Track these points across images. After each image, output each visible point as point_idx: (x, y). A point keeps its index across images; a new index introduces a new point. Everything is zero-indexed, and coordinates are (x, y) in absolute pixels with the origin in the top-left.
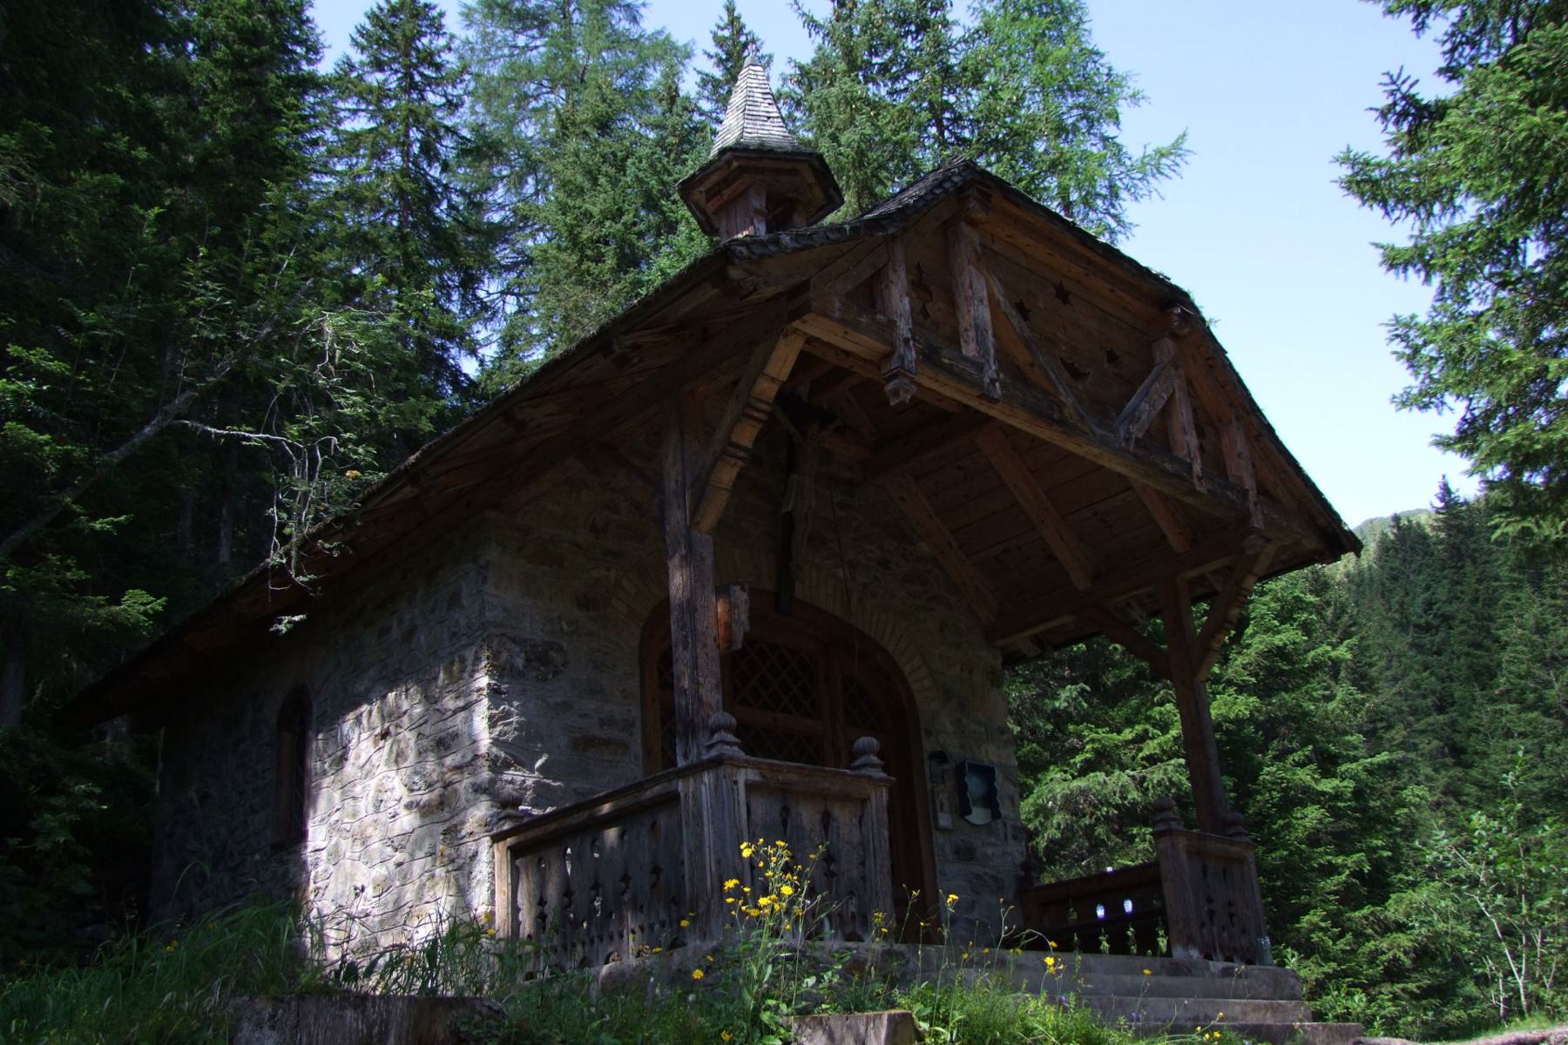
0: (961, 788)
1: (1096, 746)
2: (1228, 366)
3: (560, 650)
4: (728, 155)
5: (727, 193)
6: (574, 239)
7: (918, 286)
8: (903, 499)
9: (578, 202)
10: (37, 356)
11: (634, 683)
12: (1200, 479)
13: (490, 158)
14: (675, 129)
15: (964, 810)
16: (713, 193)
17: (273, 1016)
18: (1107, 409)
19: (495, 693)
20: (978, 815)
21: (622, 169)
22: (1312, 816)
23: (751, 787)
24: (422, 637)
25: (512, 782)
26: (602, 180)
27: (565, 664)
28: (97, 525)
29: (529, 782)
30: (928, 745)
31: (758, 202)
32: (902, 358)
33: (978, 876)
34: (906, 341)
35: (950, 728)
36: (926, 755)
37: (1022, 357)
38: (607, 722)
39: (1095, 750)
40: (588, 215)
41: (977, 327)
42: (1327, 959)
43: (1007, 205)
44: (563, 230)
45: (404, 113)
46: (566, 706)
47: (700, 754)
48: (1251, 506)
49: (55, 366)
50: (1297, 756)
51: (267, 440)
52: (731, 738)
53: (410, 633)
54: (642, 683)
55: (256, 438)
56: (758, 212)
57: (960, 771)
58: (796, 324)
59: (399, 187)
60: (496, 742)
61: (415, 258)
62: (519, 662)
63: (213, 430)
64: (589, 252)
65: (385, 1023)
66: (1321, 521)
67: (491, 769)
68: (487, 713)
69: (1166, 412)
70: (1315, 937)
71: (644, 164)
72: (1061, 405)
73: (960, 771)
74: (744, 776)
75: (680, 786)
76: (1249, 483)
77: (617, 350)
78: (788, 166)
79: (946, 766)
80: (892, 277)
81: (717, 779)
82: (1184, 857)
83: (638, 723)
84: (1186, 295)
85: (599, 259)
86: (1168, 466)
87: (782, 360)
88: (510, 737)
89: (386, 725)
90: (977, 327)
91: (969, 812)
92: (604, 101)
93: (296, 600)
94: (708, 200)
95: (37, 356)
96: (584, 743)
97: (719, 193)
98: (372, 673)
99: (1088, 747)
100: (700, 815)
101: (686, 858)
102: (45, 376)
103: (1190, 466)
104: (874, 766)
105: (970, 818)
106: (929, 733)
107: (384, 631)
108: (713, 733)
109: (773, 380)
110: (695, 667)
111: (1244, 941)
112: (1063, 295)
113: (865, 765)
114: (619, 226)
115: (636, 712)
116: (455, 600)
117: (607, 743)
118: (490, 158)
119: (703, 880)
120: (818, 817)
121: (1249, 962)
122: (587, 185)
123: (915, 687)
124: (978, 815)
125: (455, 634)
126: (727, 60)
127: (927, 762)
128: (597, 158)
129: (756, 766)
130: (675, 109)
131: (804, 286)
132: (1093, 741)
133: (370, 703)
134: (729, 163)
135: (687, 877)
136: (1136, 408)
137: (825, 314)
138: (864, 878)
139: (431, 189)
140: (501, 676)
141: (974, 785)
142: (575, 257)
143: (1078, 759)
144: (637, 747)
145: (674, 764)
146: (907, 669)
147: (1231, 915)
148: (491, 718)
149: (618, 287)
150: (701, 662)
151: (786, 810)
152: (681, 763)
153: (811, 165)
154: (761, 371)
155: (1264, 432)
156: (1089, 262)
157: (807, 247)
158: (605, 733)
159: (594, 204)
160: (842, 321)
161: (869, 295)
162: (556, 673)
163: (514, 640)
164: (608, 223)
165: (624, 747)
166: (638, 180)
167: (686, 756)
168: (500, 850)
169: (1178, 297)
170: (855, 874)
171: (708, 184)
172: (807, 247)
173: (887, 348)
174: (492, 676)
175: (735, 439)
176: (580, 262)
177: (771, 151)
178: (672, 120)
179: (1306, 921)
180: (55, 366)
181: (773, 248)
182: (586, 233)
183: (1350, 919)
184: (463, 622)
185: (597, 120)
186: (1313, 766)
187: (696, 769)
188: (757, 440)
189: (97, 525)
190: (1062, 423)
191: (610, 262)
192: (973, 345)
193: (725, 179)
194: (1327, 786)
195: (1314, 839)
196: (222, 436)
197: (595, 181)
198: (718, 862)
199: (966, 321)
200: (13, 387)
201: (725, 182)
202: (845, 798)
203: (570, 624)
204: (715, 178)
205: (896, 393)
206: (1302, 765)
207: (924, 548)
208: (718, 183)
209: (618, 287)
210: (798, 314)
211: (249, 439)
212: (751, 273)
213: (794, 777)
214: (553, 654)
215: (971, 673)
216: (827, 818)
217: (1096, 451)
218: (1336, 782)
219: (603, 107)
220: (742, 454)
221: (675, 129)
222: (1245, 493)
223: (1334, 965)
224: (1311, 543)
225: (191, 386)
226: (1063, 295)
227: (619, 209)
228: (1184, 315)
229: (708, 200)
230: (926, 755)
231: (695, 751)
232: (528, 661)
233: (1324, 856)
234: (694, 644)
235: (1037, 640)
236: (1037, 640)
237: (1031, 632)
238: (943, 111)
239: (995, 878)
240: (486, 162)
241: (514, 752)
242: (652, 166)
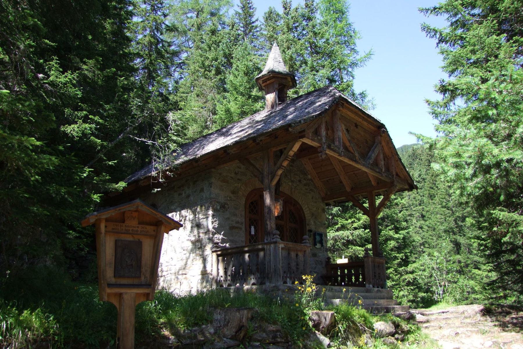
0: (315, 239)
1: (342, 223)
2: (392, 143)
3: (228, 204)
5: (268, 82)
6: (203, 64)
7: (327, 129)
8: (305, 164)
9: (205, 54)
10: (97, 118)
11: (243, 213)
13: (175, 31)
14: (233, 35)
15: (315, 244)
16: (264, 82)
17: (220, 312)
18: (364, 156)
19: (213, 216)
20: (318, 246)
21: (218, 46)
22: (392, 244)
23: (282, 248)
24: (192, 198)
25: (216, 238)
26: (212, 48)
27: (228, 208)
28: (110, 163)
29: (220, 238)
31: (276, 86)
32: (323, 147)
33: (317, 261)
34: (324, 143)
35: (313, 223)
36: (307, 230)
37: (348, 144)
38: (237, 222)
39: (341, 225)
40: (208, 58)
41: (339, 138)
42: (393, 281)
43: (347, 105)
44: (201, 62)
45: (152, 19)
46: (228, 219)
47: (271, 240)
48: (395, 179)
49: (101, 121)
50: (390, 228)
51: (152, 143)
52: (278, 237)
53: (188, 196)
54: (245, 212)
55: (150, 142)
56: (276, 89)
57: (315, 235)
58: (301, 140)
59: (150, 41)
60: (214, 228)
61: (153, 61)
62: (219, 207)
63: (138, 139)
64: (207, 69)
65: (243, 315)
66: (409, 182)
67: (212, 234)
68: (211, 221)
69: (378, 156)
70: (391, 275)
71: (225, 45)
72: (355, 156)
73: (315, 235)
74: (281, 246)
75: (265, 247)
77: (257, 141)
79: (311, 233)
80: (322, 127)
81: (275, 246)
83: (244, 223)
84: (384, 125)
85: (210, 71)
86: (377, 170)
87: (296, 147)
88: (216, 226)
89: (181, 218)
90: (339, 138)
91: (316, 245)
92: (214, 25)
93: (159, 185)
94: (263, 83)
95: (97, 118)
96: (232, 228)
97: (266, 82)
98: (176, 204)
99: (340, 224)
100: (270, 254)
101: (266, 263)
102: (97, 123)
105: (316, 246)
106: (308, 225)
107: (180, 194)
108: (274, 235)
109: (293, 151)
111: (381, 283)
112: (356, 126)
113: (305, 243)
114: (217, 63)
115: (244, 220)
116: (202, 190)
117: (237, 228)
118: (175, 31)
119: (271, 269)
120: (295, 255)
121: (382, 288)
122: (208, 49)
123: (306, 213)
124: (318, 246)
125: (202, 199)
126: (243, 8)
127: (307, 232)
128: (211, 42)
130: (234, 29)
131: (304, 131)
132: (341, 222)
133: (176, 212)
135: (266, 268)
136: (371, 155)
137: (308, 138)
138: (304, 269)
139: (158, 40)
140: (214, 211)
141: (318, 238)
142: (203, 70)
143: (337, 226)
144: (244, 229)
145: (264, 241)
146: (304, 208)
147: (379, 276)
148: (212, 222)
149: (215, 80)
151: (289, 254)
152: (266, 241)
153: (291, 77)
154: (291, 149)
155: (399, 160)
156: (363, 118)
157: (306, 122)
158: (237, 225)
159: (210, 55)
160: (312, 140)
161: (317, 133)
162: (227, 210)
163: (217, 202)
164: (214, 62)
165: (241, 229)
166: (223, 50)
167: (267, 240)
168: (214, 255)
169: (382, 126)
170: (302, 268)
172: (306, 122)
173: (320, 145)
174: (212, 211)
175: (283, 164)
176: (205, 71)
177: (281, 73)
178: (232, 32)
179: (389, 271)
180: (101, 121)
181: (299, 124)
182: (207, 63)
183: (399, 270)
184: (204, 196)
185: (211, 30)
186: (394, 231)
187: (270, 243)
188: (287, 165)
189: (110, 163)
190: (356, 161)
191: (213, 72)
192: (338, 142)
194: (396, 236)
195: (392, 250)
196: (140, 140)
197: (210, 49)
198: (275, 266)
200: (90, 126)
201: (268, 79)
202: (301, 251)
203: (230, 198)
206: (390, 230)
207: (309, 177)
208: (266, 79)
209: (215, 80)
210: (302, 137)
211: (147, 142)
212: (294, 129)
214: (226, 206)
215: (318, 209)
216: (297, 255)
217: (362, 167)
218: (399, 235)
219: (213, 27)
220: (284, 168)
221: (233, 35)
222: (393, 176)
223: (395, 282)
224: (407, 187)
225: (131, 126)
226: (356, 126)
227: (217, 57)
228: (384, 132)
229: (263, 83)
230: (307, 230)
231: (269, 239)
232: (220, 207)
233: (394, 254)
235: (335, 202)
236: (335, 202)
237: (333, 200)
238: (313, 43)
239: (321, 261)
240: (173, 33)
241: (218, 231)
242: (227, 46)
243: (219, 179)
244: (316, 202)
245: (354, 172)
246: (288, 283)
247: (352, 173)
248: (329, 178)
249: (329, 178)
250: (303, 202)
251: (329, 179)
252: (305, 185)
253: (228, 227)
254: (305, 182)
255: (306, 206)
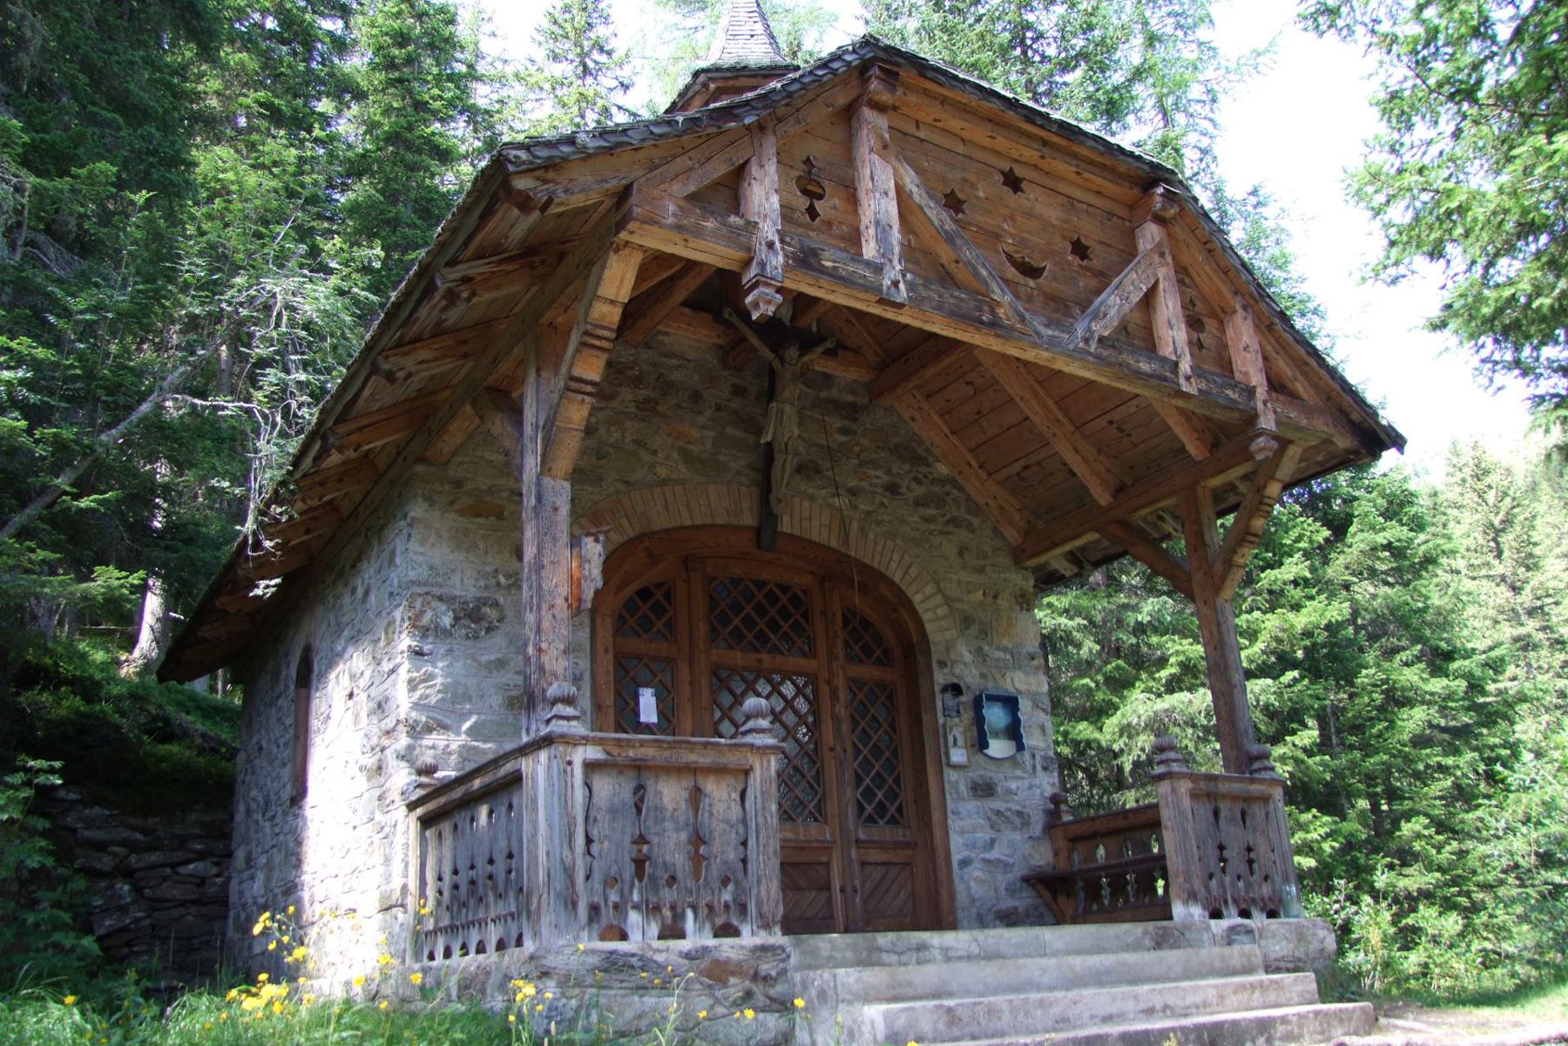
0: (979, 720)
1: (1181, 658)
3: (496, 604)
4: (702, 78)
12: (1188, 378)
15: (980, 743)
20: (998, 748)
22: (1414, 719)
23: (591, 767)
25: (433, 747)
29: (454, 746)
30: (940, 678)
32: (763, 265)
33: (998, 813)
35: (968, 657)
39: (1181, 664)
41: (877, 223)
42: (1430, 870)
47: (538, 730)
48: (1260, 406)
49: (41, 353)
50: (1404, 656)
51: (241, 408)
58: (623, 235)
60: (416, 706)
62: (447, 621)
66: (1355, 416)
70: (1417, 846)
72: (993, 305)
73: (977, 705)
76: (1258, 380)
82: (1187, 802)
88: (433, 700)
90: (877, 223)
91: (986, 746)
99: (1172, 660)
102: (36, 364)
103: (1176, 364)
104: (763, 731)
105: (989, 752)
106: (942, 664)
107: (354, 590)
109: (612, 302)
110: (539, 631)
111: (1266, 890)
112: (1013, 183)
120: (685, 794)
121: (1272, 914)
123: (926, 617)
124: (998, 748)
127: (939, 698)
129: (599, 742)
132: (1177, 653)
134: (705, 85)
141: (995, 716)
143: (1164, 674)
146: (916, 599)
147: (1250, 862)
148: (410, 681)
150: (545, 625)
151: (640, 789)
156: (1045, 143)
160: (678, 228)
162: (489, 630)
163: (440, 598)
173: (741, 255)
179: (1407, 829)
180: (41, 353)
183: (1462, 822)
186: (1423, 665)
189: (82, 505)
194: (1437, 685)
195: (1420, 741)
199: (867, 215)
202: (720, 771)
203: (508, 577)
205: (756, 305)
206: (1407, 664)
207: (942, 469)
211: (224, 408)
212: (545, 181)
213: (650, 752)
214: (487, 610)
215: (995, 597)
216: (696, 795)
217: (1045, 354)
218: (1444, 682)
220: (589, 389)
222: (1251, 392)
223: (1438, 875)
224: (1343, 442)
228: (1169, 197)
230: (937, 688)
232: (457, 619)
233: (1433, 755)
234: (539, 608)
235: (1073, 557)
236: (1073, 557)
239: (1019, 814)
243: (451, 503)
244: (981, 570)
245: (1108, 417)
246: (635, 935)
247: (1102, 422)
248: (1021, 463)
249: (1021, 463)
250: (913, 572)
251: (1026, 468)
252: (919, 503)
253: (496, 701)
254: (919, 491)
255: (929, 590)
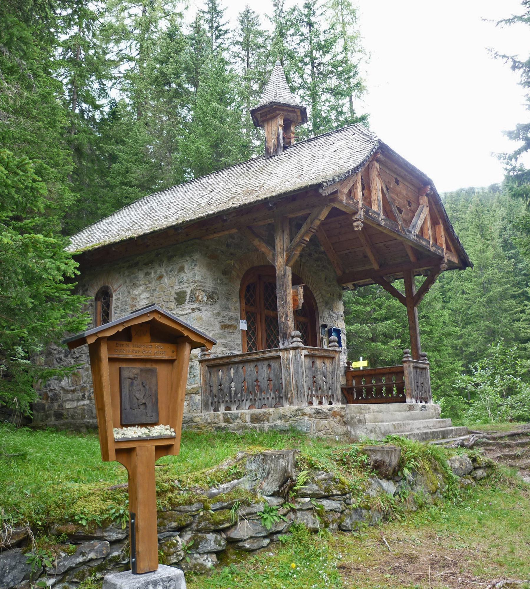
3: (216, 294)
4: (272, 104)
11: (238, 304)
12: (432, 247)
23: (305, 356)
30: (321, 323)
36: (320, 325)
38: (231, 319)
41: (378, 200)
46: (219, 314)
47: (288, 344)
52: (299, 340)
54: (240, 304)
74: (304, 352)
76: (444, 246)
78: (293, 109)
81: (296, 353)
90: (378, 200)
103: (429, 242)
104: (336, 346)
108: (293, 338)
109: (320, 220)
110: (287, 315)
123: (318, 301)
129: (307, 349)
134: (272, 106)
146: (315, 295)
150: (288, 313)
151: (313, 362)
152: (281, 347)
154: (316, 218)
162: (215, 302)
167: (283, 344)
171: (262, 112)
192: (376, 206)
193: (269, 111)
199: (374, 197)
204: (265, 110)
205: (357, 226)
207: (322, 249)
213: (316, 352)
214: (215, 295)
220: (306, 242)
222: (443, 250)
232: (208, 298)
234: (286, 307)
244: (330, 286)
245: (384, 243)
246: (314, 404)
247: (382, 244)
248: (349, 251)
249: (349, 251)
250: (314, 286)
251: (349, 252)
252: (316, 260)
253: (218, 326)
254: (316, 255)
255: (318, 292)
